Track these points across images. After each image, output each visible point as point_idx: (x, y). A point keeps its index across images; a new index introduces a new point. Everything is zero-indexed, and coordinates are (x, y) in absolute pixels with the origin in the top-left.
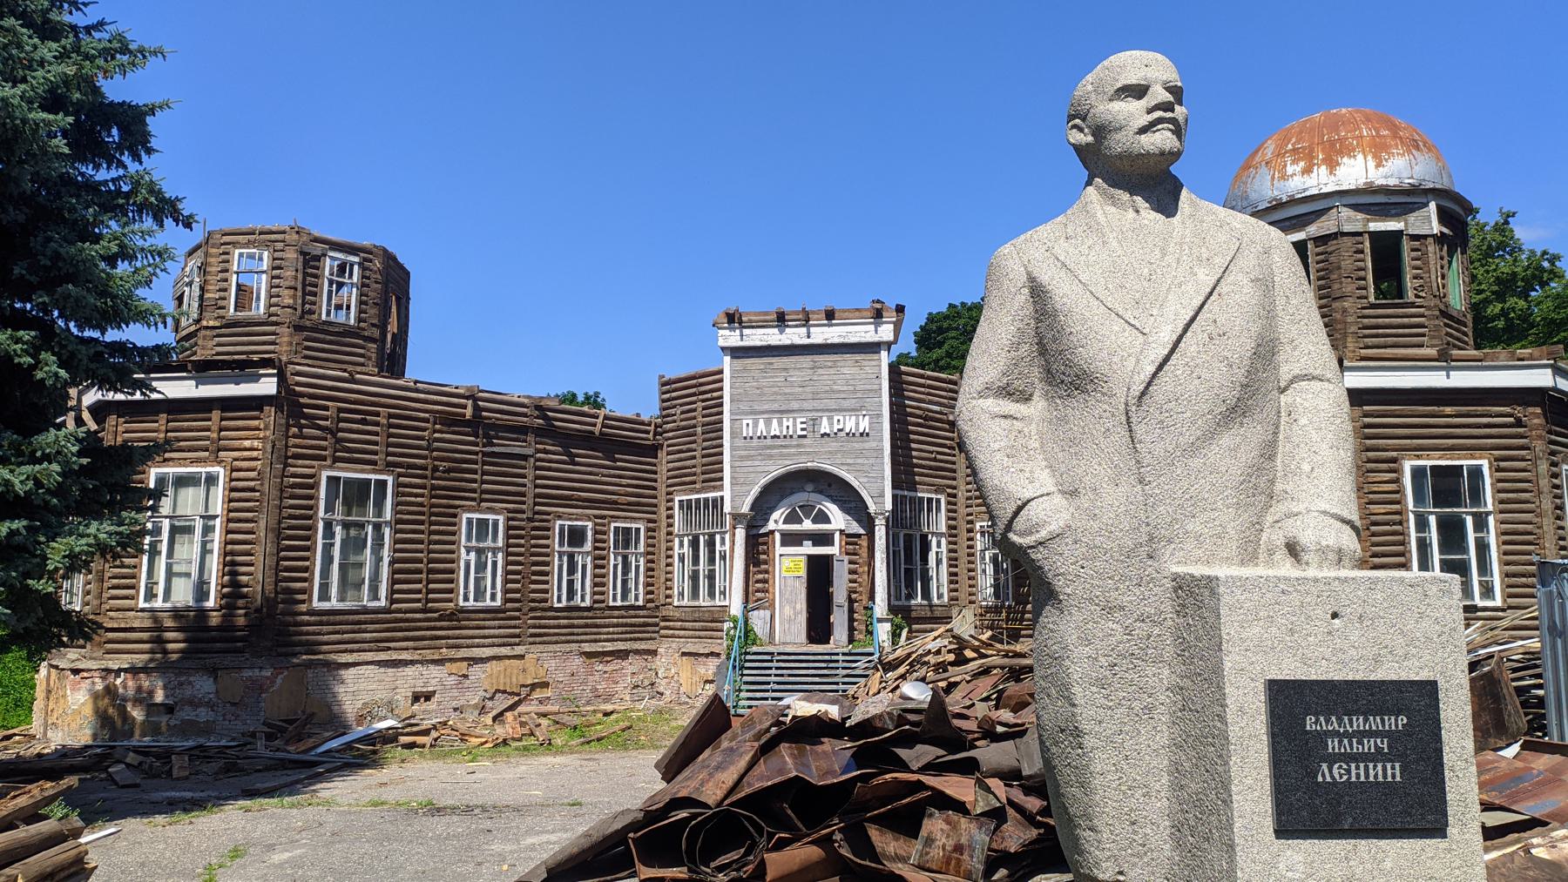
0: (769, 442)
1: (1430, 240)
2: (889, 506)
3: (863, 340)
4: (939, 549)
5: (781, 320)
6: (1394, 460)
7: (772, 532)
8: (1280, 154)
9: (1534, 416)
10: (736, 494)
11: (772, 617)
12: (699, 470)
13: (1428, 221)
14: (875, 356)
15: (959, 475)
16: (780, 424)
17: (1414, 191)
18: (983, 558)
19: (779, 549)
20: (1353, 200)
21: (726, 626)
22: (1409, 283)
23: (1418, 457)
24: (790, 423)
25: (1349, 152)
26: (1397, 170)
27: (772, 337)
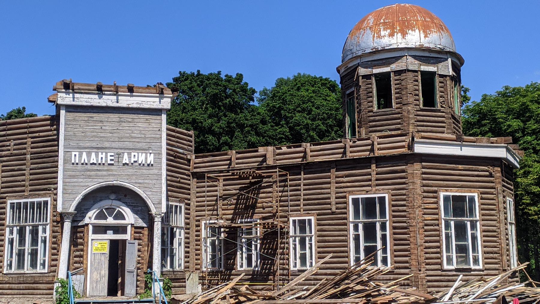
0: (89, 167)
1: (448, 78)
2: (164, 210)
3: (152, 107)
4: (180, 236)
5: (100, 90)
6: (435, 192)
7: (87, 225)
8: (377, 24)
9: (497, 171)
10: (66, 201)
11: (85, 279)
12: (27, 183)
13: (446, 68)
14: (158, 117)
15: (192, 192)
16: (97, 156)
17: (441, 51)
18: (206, 243)
19: (91, 236)
20: (414, 53)
21: (56, 285)
22: (438, 100)
23: (447, 191)
24: (104, 156)
25: (412, 28)
26: (433, 40)
27: (94, 100)
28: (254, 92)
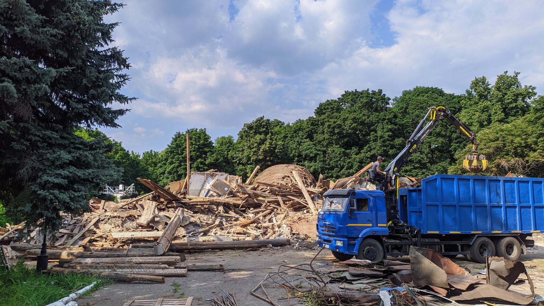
28: (389, 99)
